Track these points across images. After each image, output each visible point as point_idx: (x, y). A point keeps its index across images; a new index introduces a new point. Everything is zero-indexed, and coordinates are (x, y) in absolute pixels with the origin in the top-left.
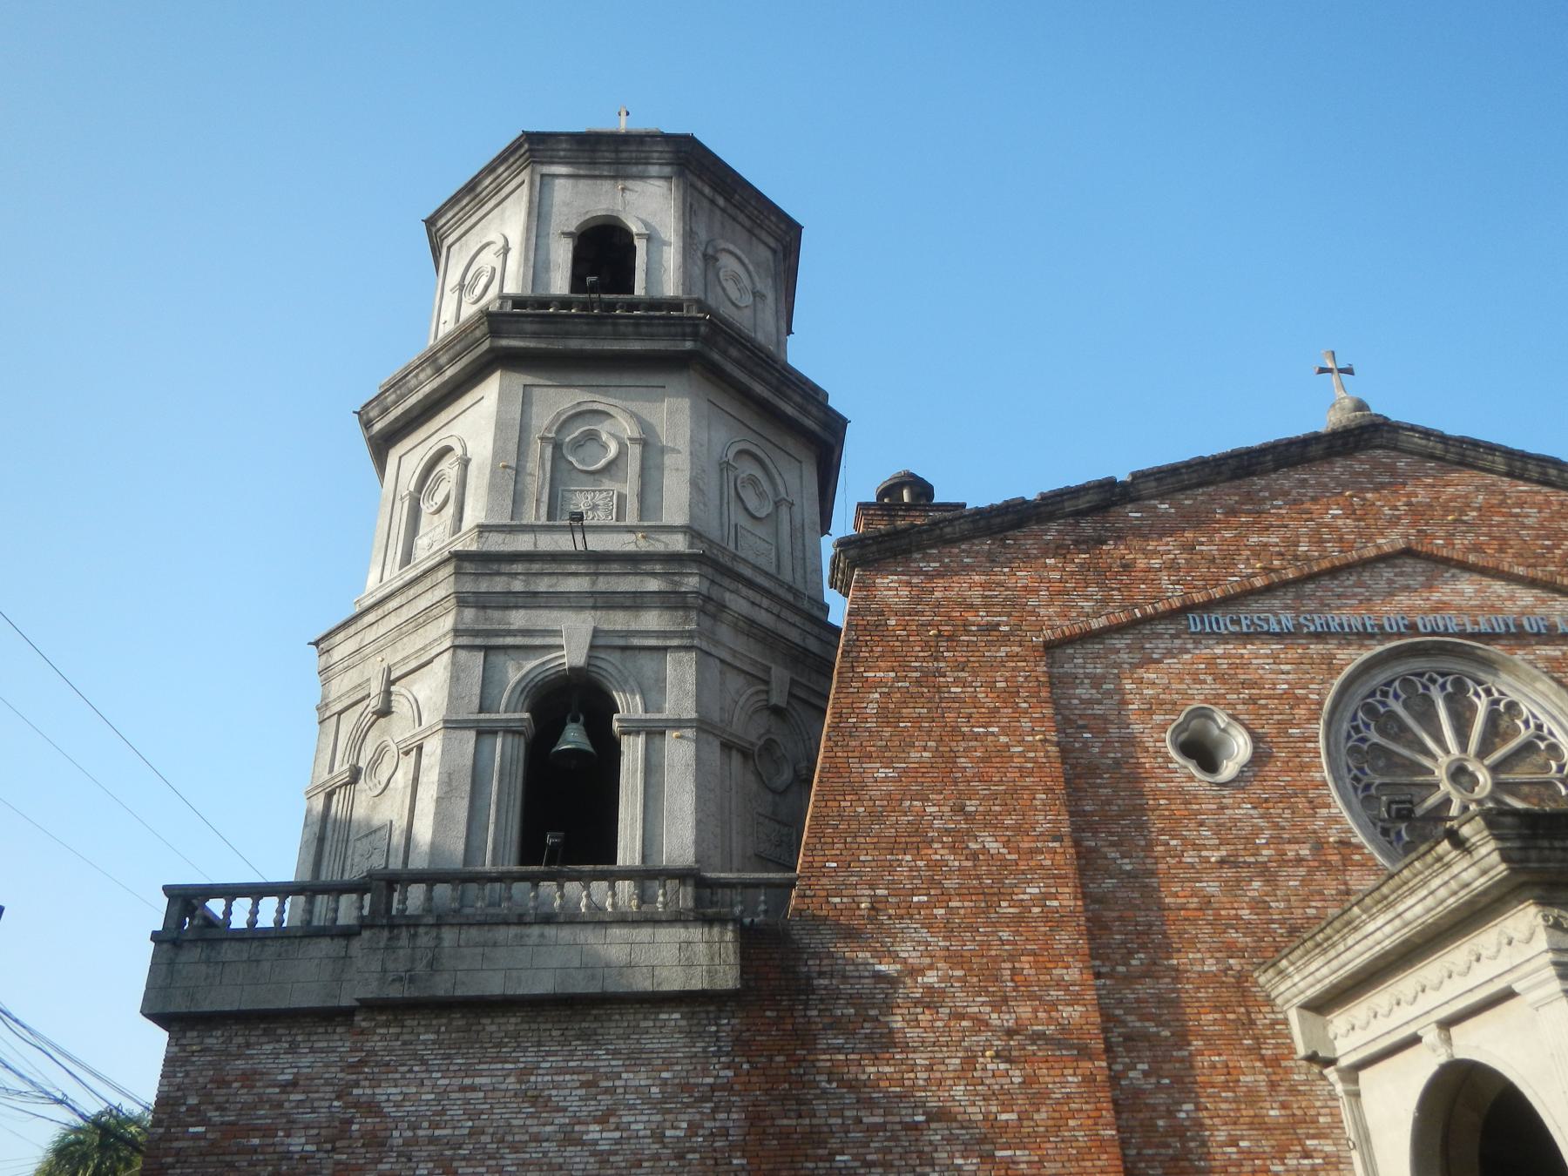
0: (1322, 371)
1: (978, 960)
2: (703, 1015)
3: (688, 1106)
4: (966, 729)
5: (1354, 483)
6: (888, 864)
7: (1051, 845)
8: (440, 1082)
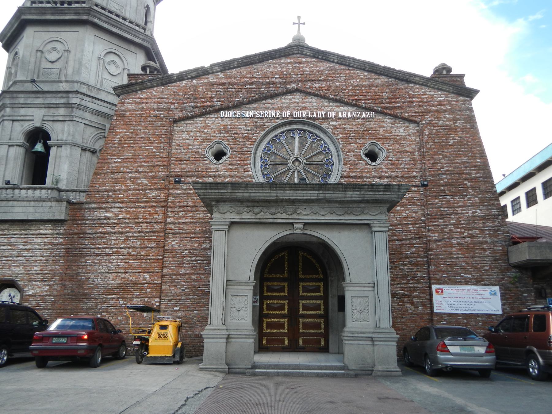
0: (294, 23)
1: (134, 213)
2: (57, 225)
3: (50, 248)
4: (144, 147)
5: (286, 66)
6: (113, 186)
7: (161, 181)
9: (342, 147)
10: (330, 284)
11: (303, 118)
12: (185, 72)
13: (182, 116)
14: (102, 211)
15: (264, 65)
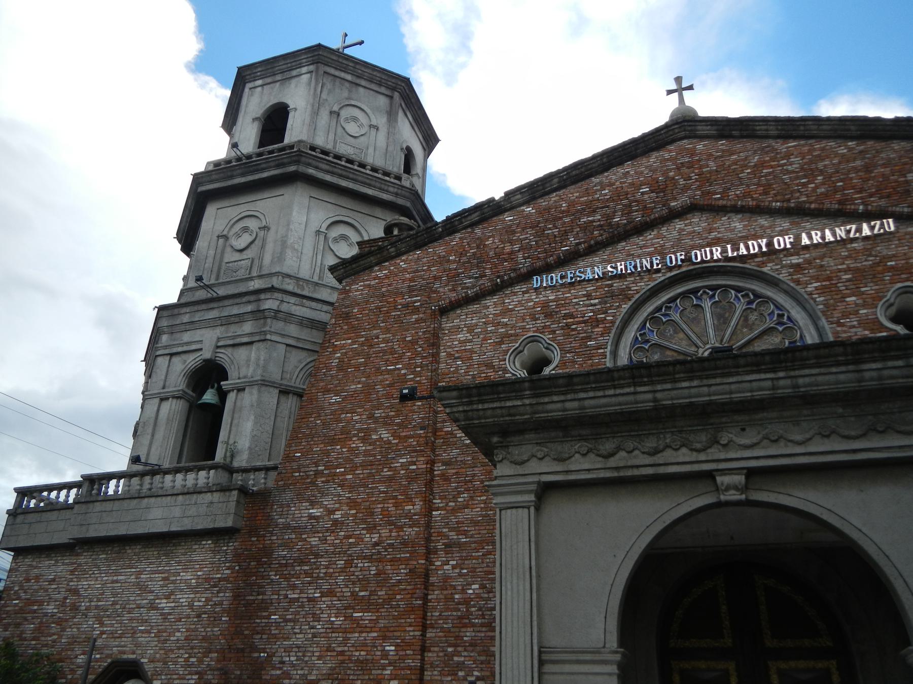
0: (670, 92)
2: (222, 541)
3: (207, 589)
5: (662, 167)
8: (104, 579)
9: (825, 309)
11: (718, 260)
12: (457, 217)
13: (457, 298)
14: (304, 504)
15: (615, 175)
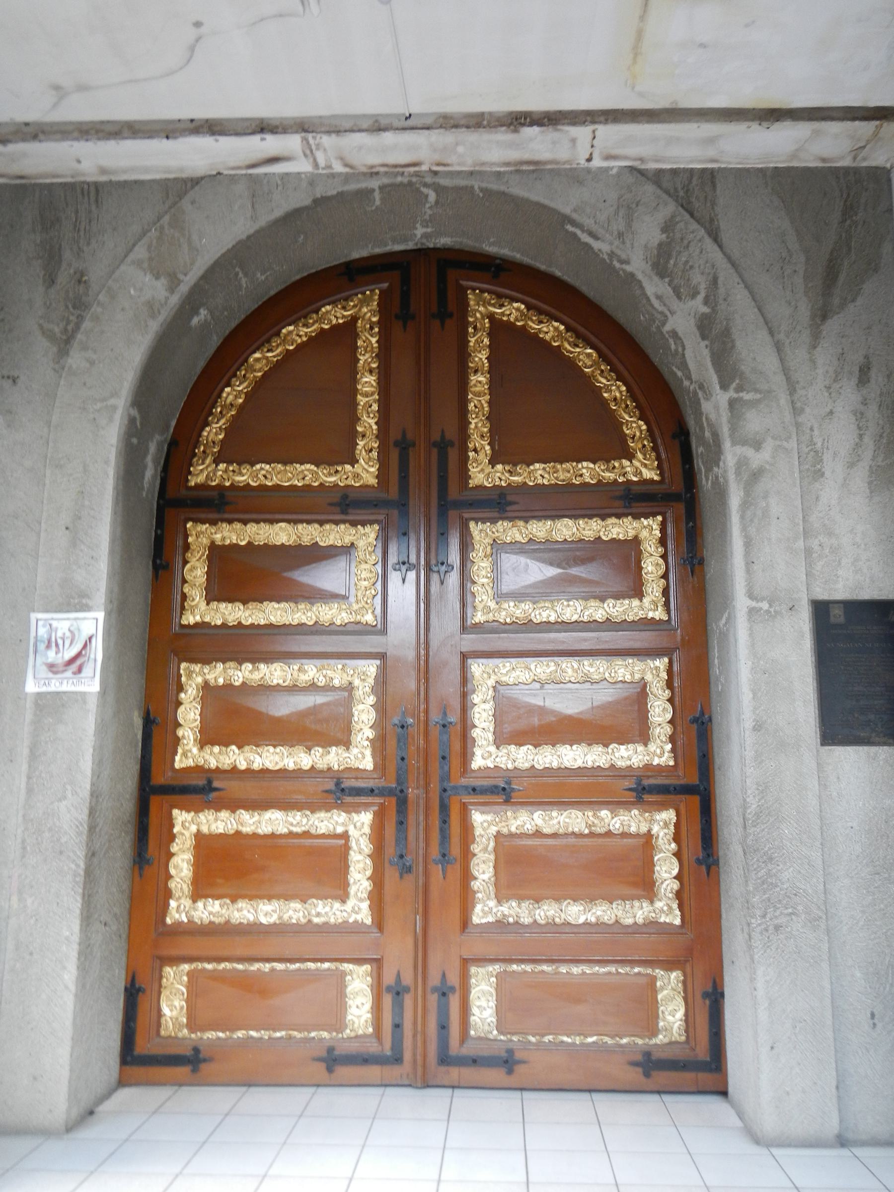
10: (735, 501)
